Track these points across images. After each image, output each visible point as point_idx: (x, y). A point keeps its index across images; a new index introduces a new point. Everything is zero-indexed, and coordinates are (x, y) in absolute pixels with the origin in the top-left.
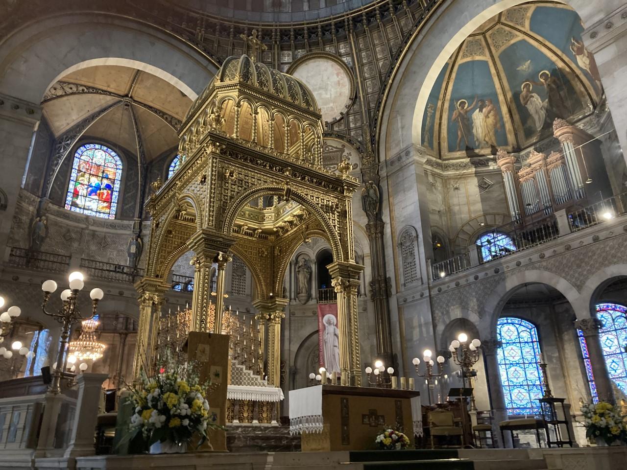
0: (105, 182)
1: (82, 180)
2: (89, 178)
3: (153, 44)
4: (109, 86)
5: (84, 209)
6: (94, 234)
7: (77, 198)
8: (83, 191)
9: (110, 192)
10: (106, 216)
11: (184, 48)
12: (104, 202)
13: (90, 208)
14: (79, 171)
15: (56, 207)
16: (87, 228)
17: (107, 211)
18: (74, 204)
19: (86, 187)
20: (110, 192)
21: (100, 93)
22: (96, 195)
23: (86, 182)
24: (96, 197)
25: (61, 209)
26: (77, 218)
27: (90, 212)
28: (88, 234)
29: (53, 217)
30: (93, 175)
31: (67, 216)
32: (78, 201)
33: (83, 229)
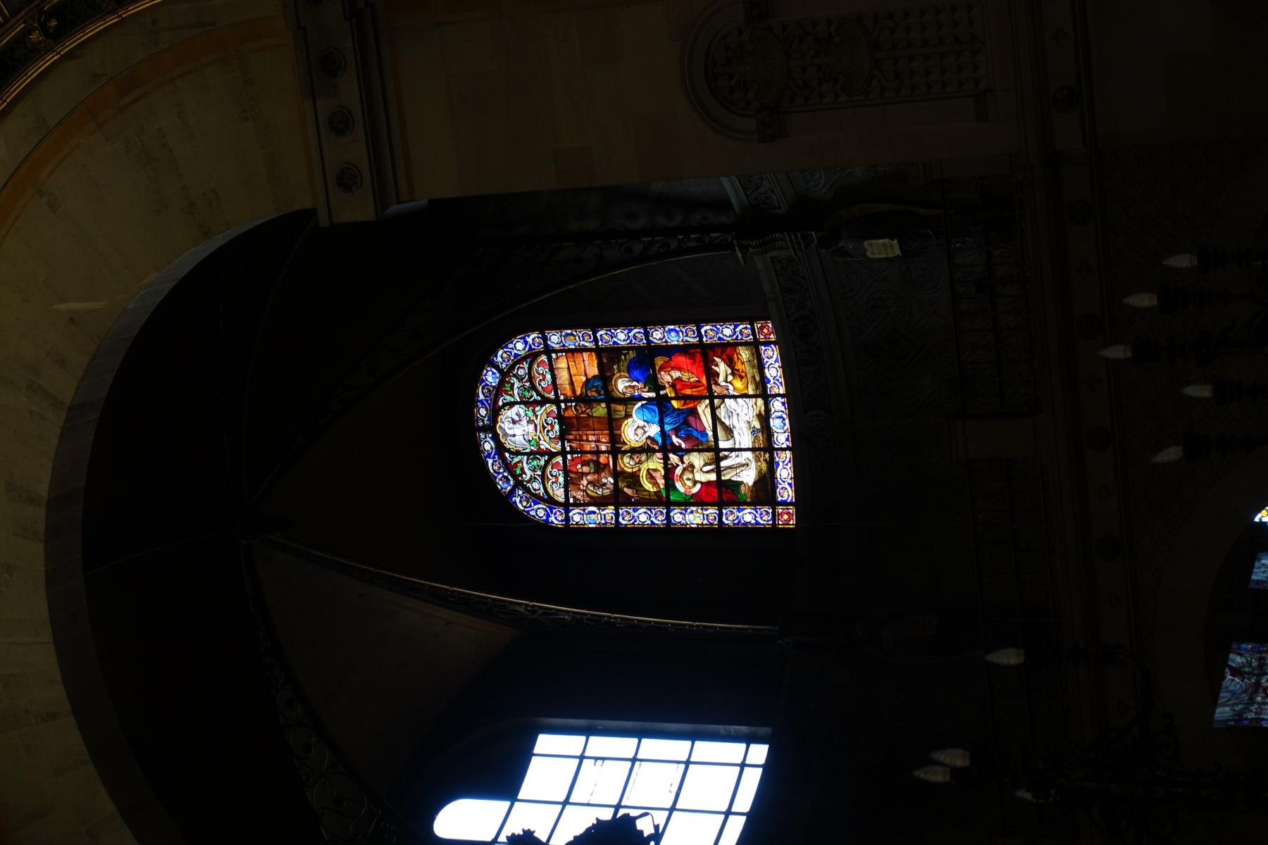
1: (651, 477)
2: (634, 451)
7: (740, 483)
9: (659, 361)
10: (772, 356)
12: (712, 376)
13: (758, 426)
14: (617, 499)
17: (744, 354)
18: (764, 491)
19: (674, 458)
20: (659, 361)
22: (694, 412)
23: (656, 463)
24: (703, 409)
27: (775, 424)
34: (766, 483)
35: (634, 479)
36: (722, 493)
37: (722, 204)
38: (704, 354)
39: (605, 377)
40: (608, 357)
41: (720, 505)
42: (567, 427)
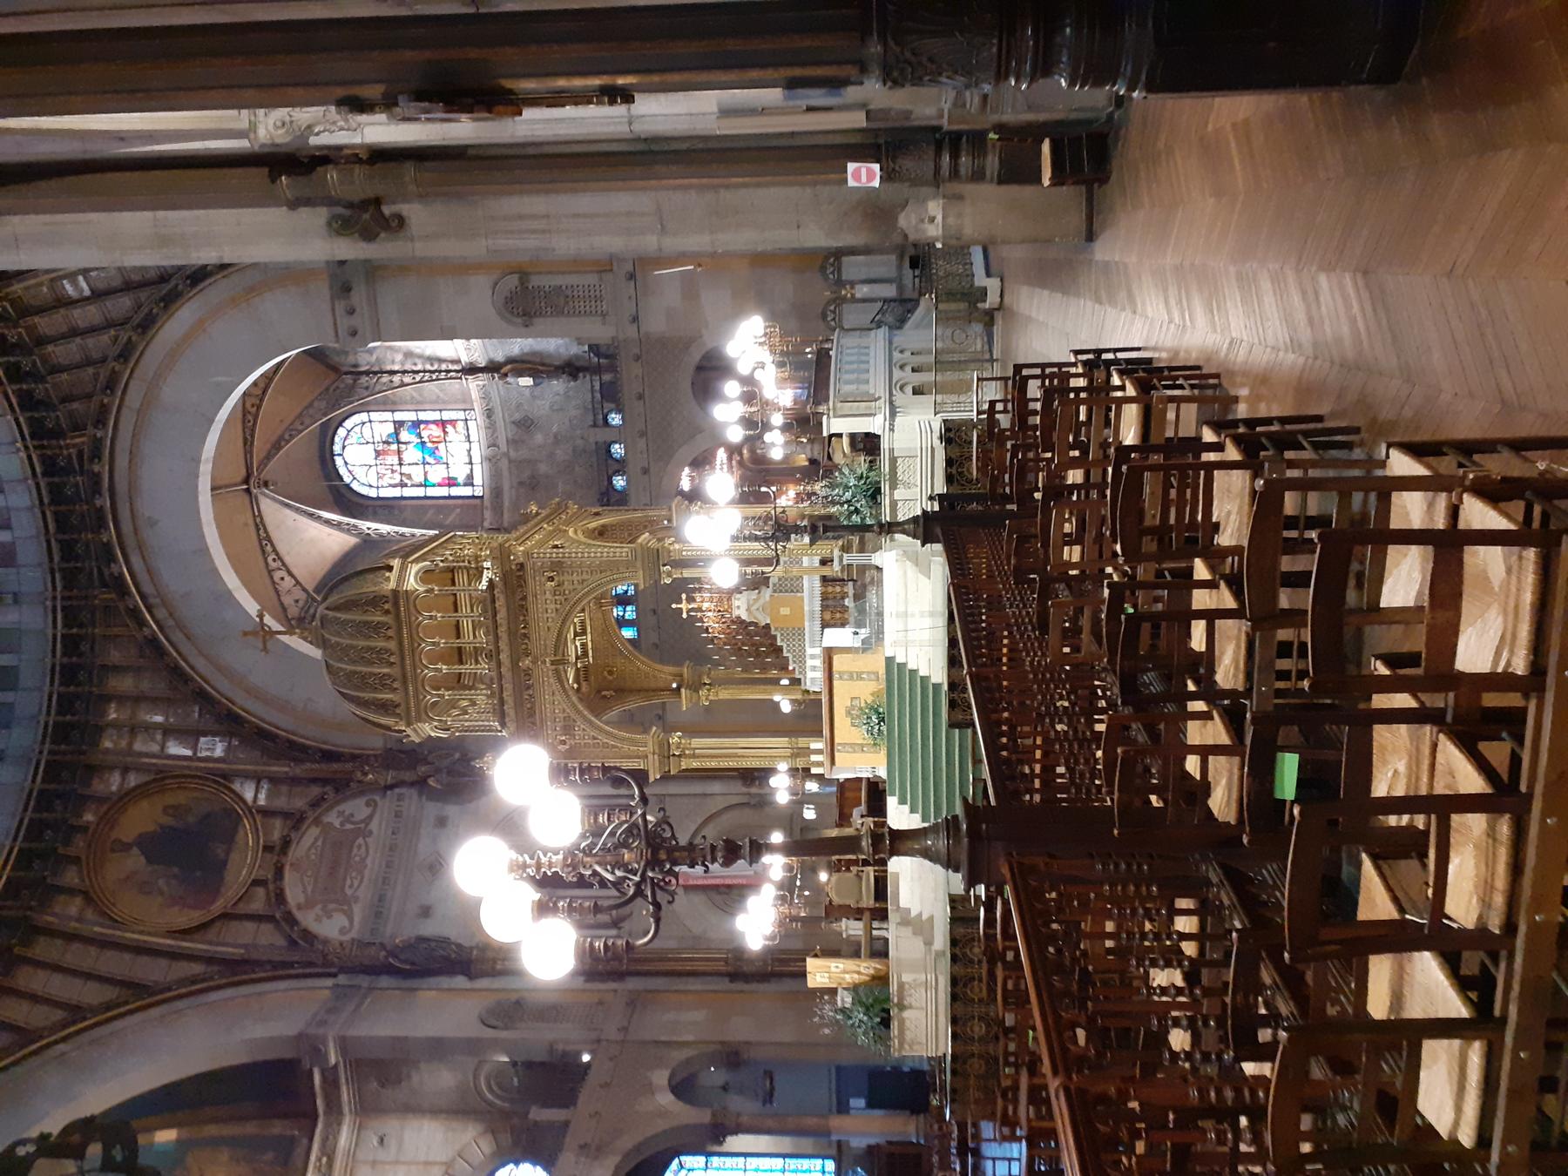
0: (405, 435)
3: (152, 523)
4: (246, 524)
5: (471, 463)
6: (513, 442)
8: (437, 473)
11: (122, 462)
12: (445, 433)
14: (403, 485)
15: (488, 514)
16: (506, 455)
17: (460, 425)
18: (469, 482)
21: (266, 531)
24: (441, 446)
25: (487, 502)
26: (495, 476)
28: (517, 450)
29: (506, 516)
30: (400, 459)
31: (496, 491)
32: (460, 473)
33: (510, 461)
34: (470, 477)
35: (409, 477)
36: (451, 482)
37: (458, 362)
38: (442, 424)
39: (397, 433)
40: (399, 425)
41: (450, 485)
42: (378, 453)
